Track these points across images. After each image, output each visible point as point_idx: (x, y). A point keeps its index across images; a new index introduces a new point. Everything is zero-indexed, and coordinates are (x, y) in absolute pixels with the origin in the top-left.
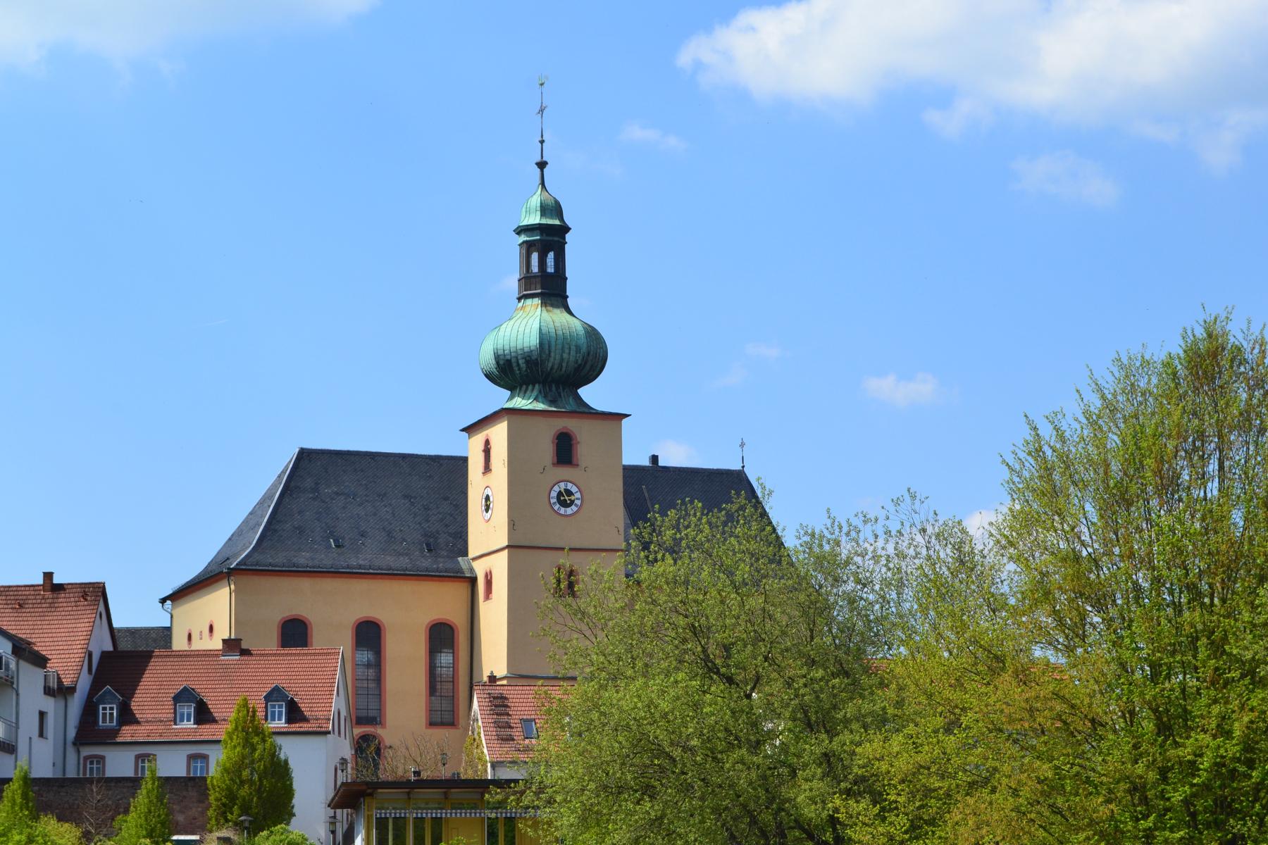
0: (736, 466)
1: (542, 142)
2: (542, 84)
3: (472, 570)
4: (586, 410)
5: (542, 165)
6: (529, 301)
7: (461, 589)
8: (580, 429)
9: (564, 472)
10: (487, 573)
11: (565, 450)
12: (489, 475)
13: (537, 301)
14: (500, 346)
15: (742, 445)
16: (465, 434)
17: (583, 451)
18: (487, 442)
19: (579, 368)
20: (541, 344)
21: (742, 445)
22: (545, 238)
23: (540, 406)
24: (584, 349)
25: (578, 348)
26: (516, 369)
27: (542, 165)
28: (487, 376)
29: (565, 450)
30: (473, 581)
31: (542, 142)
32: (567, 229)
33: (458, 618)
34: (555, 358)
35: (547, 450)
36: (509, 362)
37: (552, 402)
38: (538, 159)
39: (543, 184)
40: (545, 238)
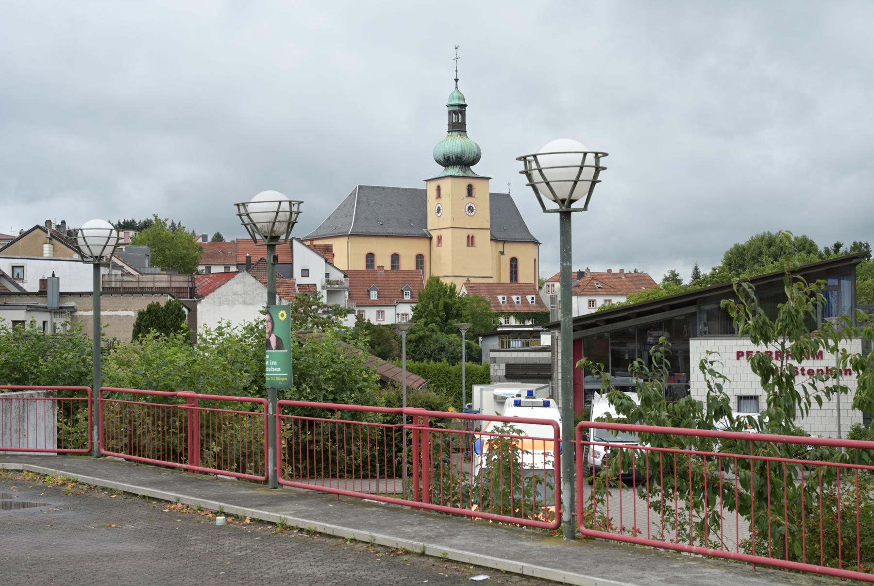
0: (507, 193)
1: (456, 71)
2: (456, 48)
3: (430, 234)
4: (475, 176)
5: (457, 80)
6: (454, 133)
7: (427, 242)
8: (476, 184)
9: (470, 199)
10: (438, 237)
11: (470, 190)
12: (439, 199)
13: (457, 133)
14: (446, 151)
15: (509, 184)
16: (425, 182)
17: (476, 192)
18: (439, 187)
19: (473, 161)
20: (462, 151)
21: (509, 184)
22: (459, 109)
23: (461, 174)
24: (476, 153)
25: (474, 152)
26: (451, 160)
27: (457, 80)
28: (437, 161)
29: (470, 190)
30: (431, 238)
31: (456, 71)
32: (466, 105)
33: (425, 253)
34: (467, 155)
35: (465, 191)
36: (449, 157)
37: (464, 172)
38: (455, 78)
39: (457, 87)
40: (459, 109)
